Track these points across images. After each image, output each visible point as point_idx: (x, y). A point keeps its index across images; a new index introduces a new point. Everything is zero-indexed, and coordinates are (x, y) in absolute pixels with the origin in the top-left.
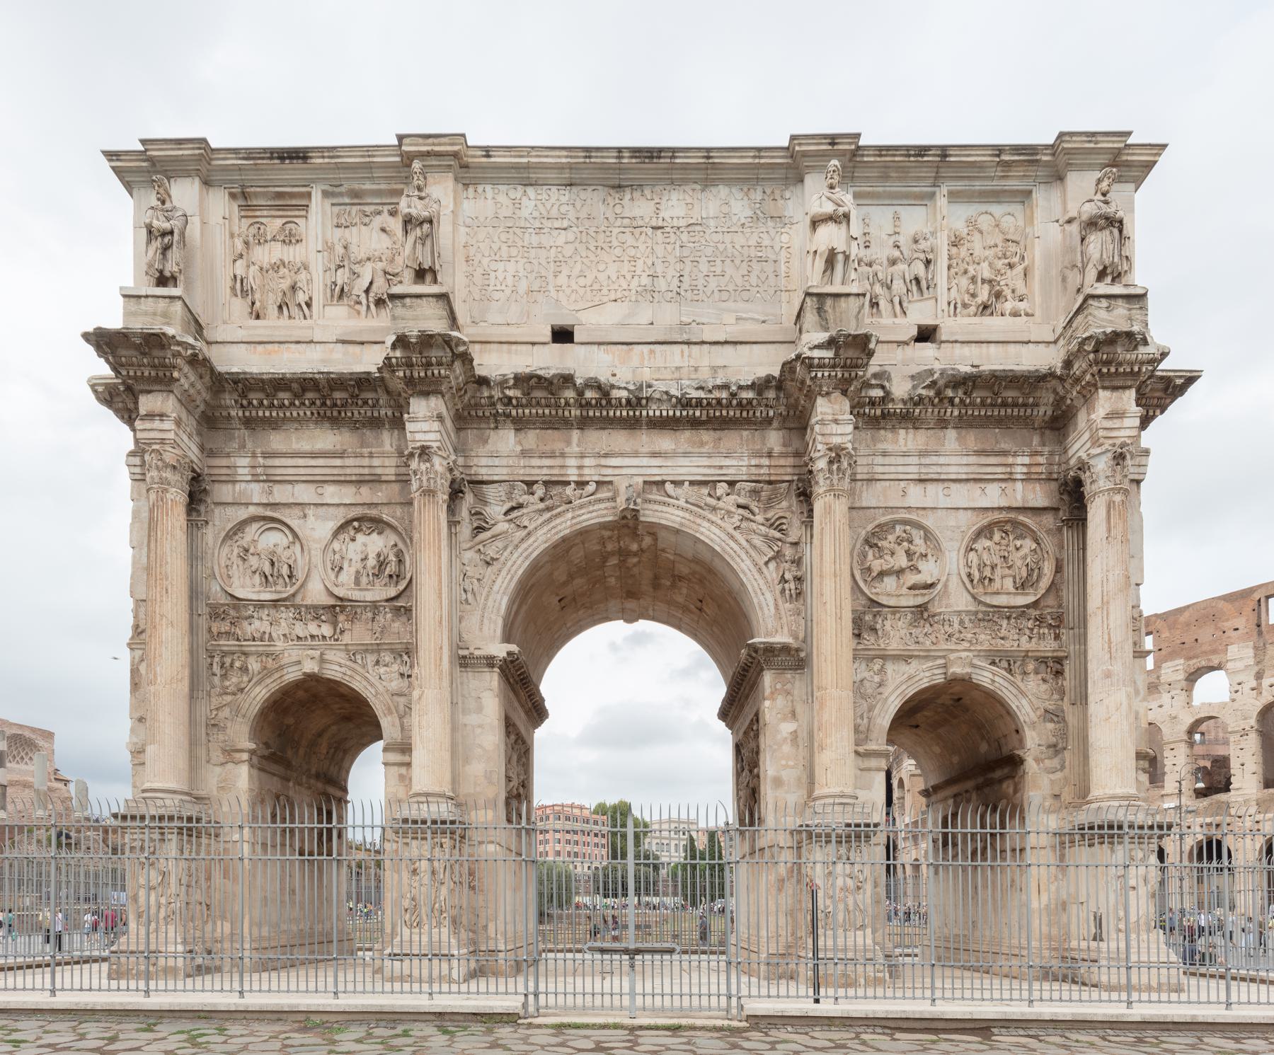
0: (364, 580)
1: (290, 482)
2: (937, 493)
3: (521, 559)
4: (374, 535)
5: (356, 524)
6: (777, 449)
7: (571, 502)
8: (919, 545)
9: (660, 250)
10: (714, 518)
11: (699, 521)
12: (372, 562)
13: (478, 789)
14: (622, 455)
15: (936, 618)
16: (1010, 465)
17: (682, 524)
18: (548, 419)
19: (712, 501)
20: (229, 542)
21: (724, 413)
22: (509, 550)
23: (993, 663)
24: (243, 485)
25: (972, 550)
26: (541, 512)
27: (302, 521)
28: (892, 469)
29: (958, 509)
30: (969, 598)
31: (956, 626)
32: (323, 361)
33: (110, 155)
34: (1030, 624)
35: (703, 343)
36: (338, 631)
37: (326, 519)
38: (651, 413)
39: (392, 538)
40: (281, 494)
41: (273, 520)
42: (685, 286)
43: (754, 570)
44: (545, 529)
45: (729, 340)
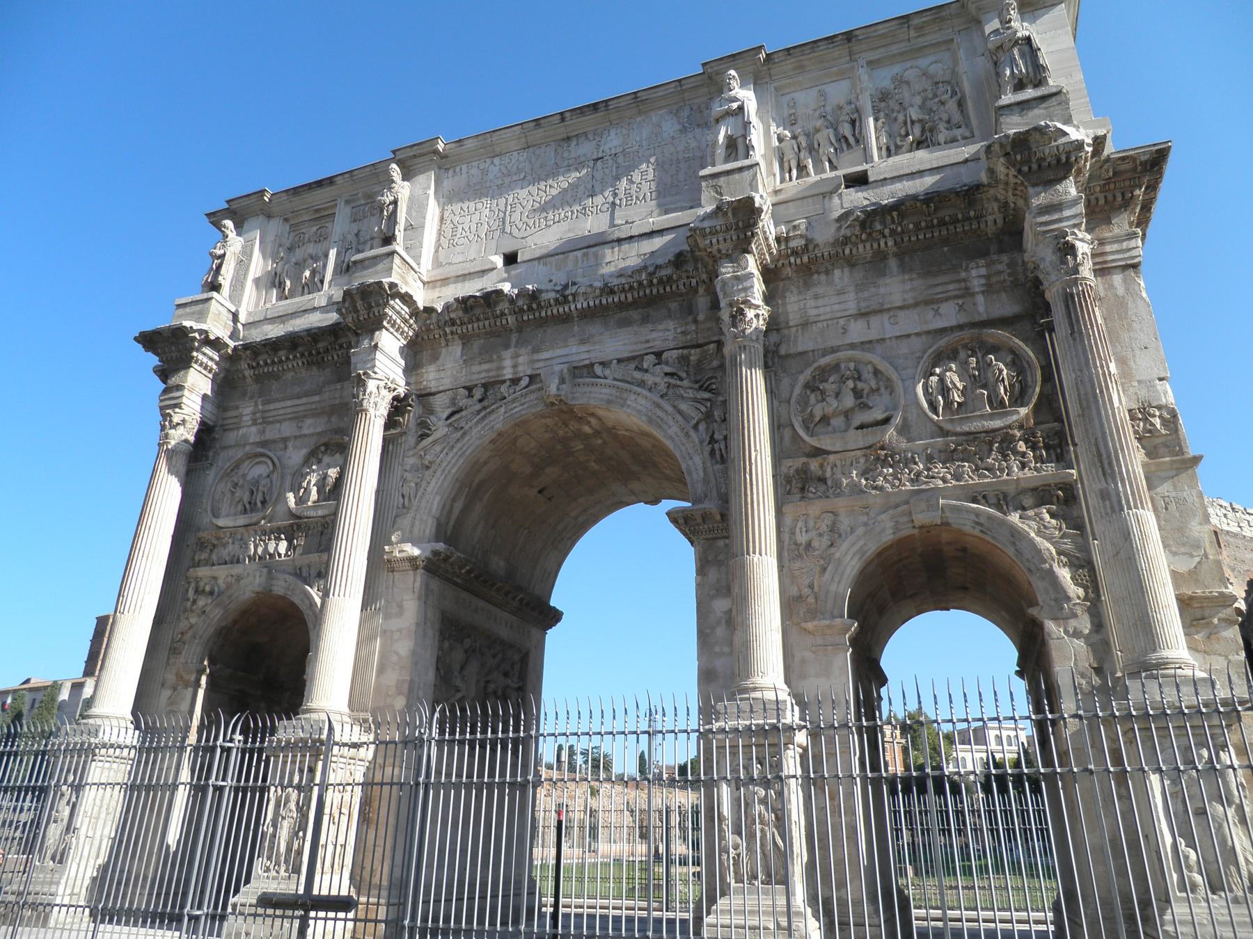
1: (279, 421)
5: (323, 448)
7: (505, 398)
9: (598, 175)
11: (625, 395)
16: (964, 280)
18: (488, 329)
21: (648, 291)
22: (445, 452)
23: (975, 500)
24: (245, 429)
26: (479, 412)
27: (282, 452)
28: (828, 309)
29: (908, 336)
33: (208, 215)
38: (579, 306)
40: (271, 433)
41: (262, 455)
45: (655, 229)
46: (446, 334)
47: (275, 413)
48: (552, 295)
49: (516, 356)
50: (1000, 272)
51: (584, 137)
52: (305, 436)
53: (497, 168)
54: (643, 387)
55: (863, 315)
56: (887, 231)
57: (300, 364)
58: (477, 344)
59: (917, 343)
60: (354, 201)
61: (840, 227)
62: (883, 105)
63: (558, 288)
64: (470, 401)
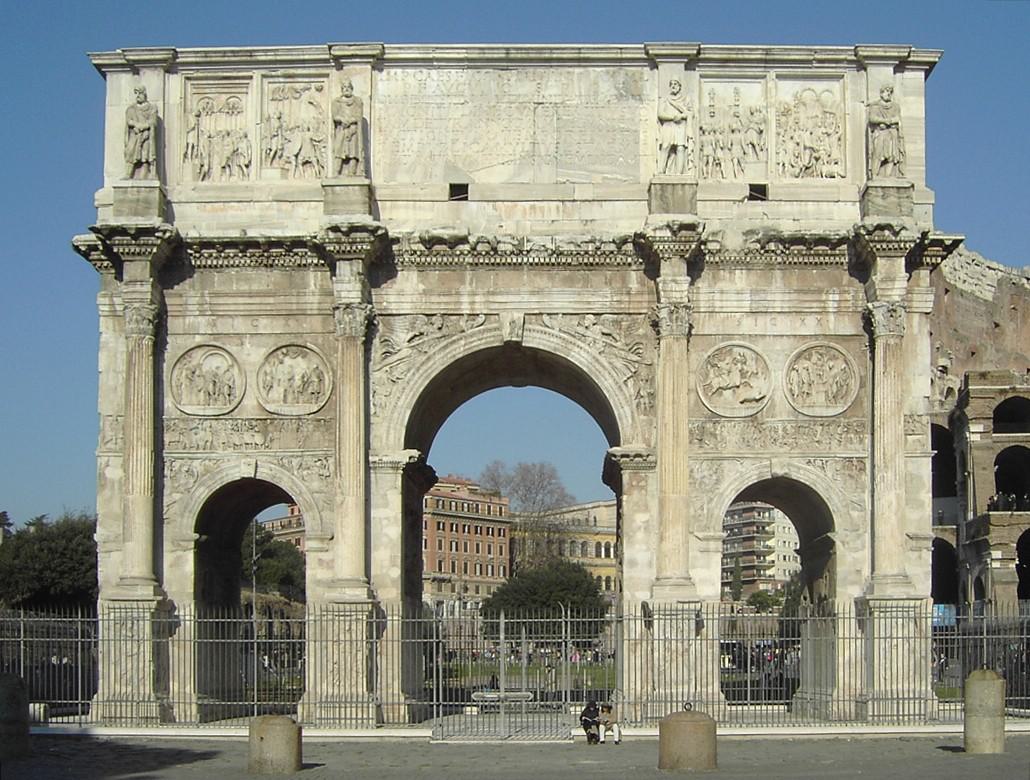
0: (290, 398)
1: (230, 316)
2: (765, 324)
3: (423, 378)
4: (299, 359)
5: (284, 350)
6: (634, 285)
7: (463, 331)
8: (751, 366)
9: (540, 123)
10: (582, 345)
11: (570, 346)
12: (298, 382)
13: (384, 571)
14: (508, 293)
15: (764, 426)
16: (824, 301)
17: (555, 349)
19: (581, 330)
25: (794, 369)
27: (240, 348)
31: (780, 432)
32: (260, 216)
34: (839, 430)
35: (574, 201)
36: (269, 439)
37: (259, 346)
38: (531, 260)
39: (315, 361)
40: (224, 326)
42: (561, 152)
43: (615, 387)
44: (442, 354)
47: (226, 308)
48: (509, 248)
56: (779, 252)
57: (248, 261)
58: (434, 275)
59: (786, 343)
60: (272, 77)
61: (746, 240)
62: (783, 119)
63: (516, 243)
64: (431, 329)
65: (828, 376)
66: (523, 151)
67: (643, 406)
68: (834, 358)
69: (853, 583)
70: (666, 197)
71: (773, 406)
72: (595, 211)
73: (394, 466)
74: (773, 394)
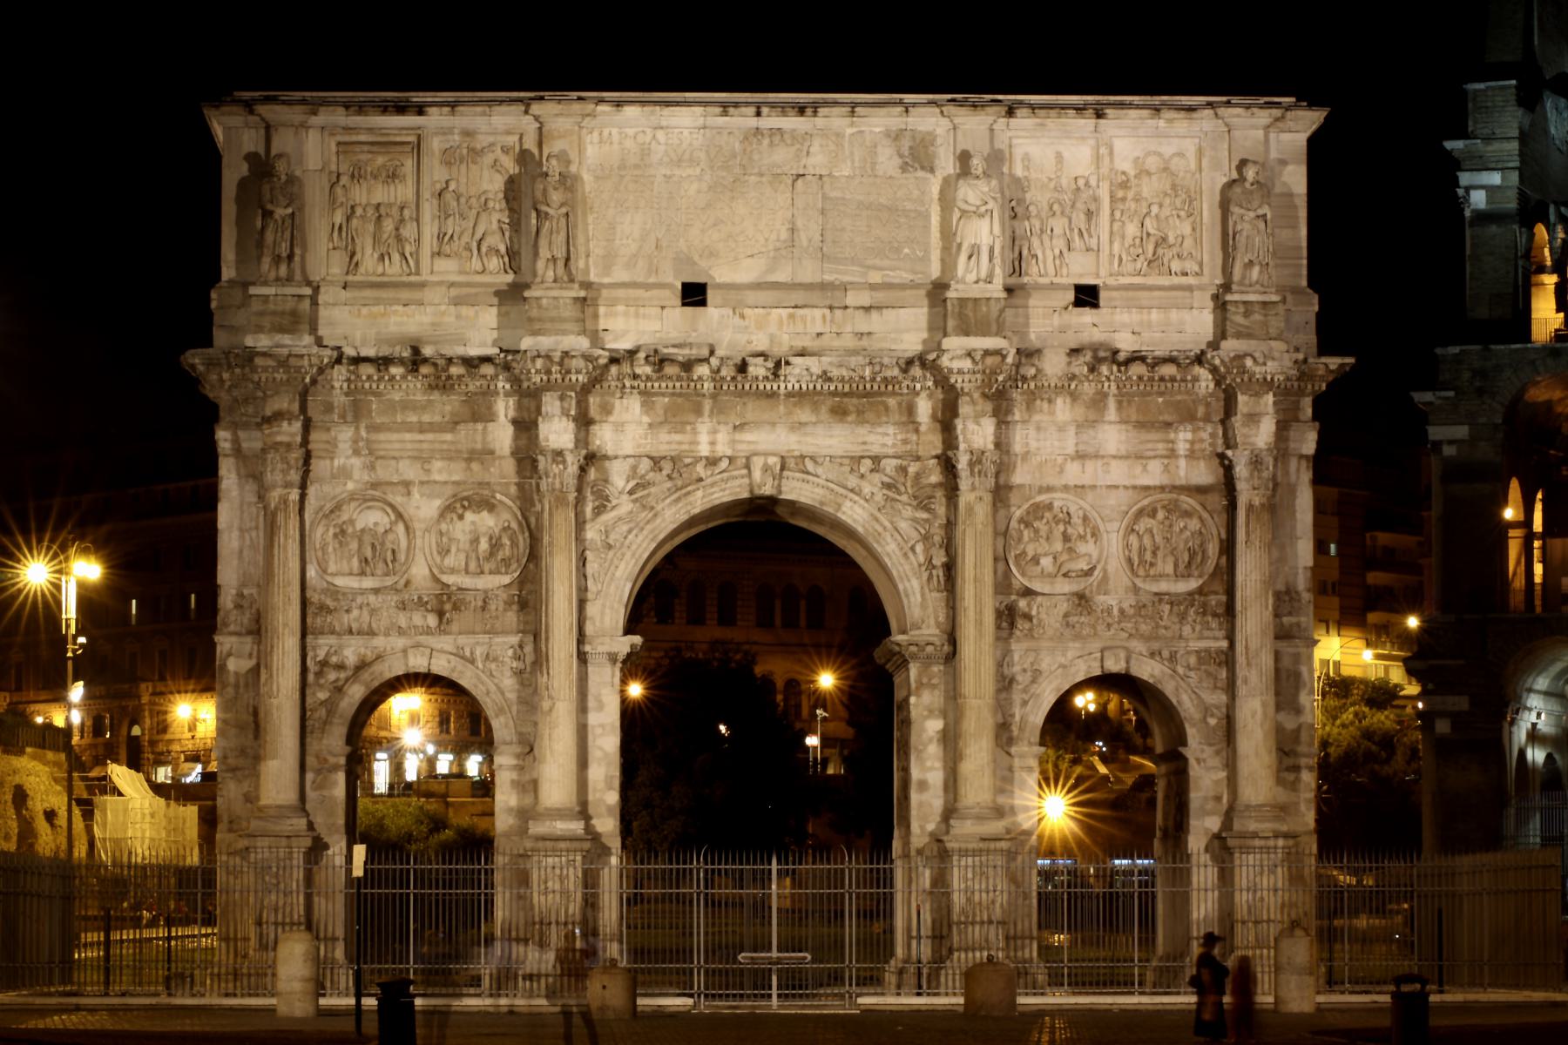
1: (394, 458)
4: (485, 514)
5: (466, 503)
7: (701, 480)
12: (484, 545)
16: (1172, 442)
17: (822, 503)
20: (323, 522)
21: (868, 386)
22: (634, 532)
27: (405, 499)
29: (1117, 487)
30: (1130, 584)
31: (1115, 611)
32: (433, 324)
35: (846, 307)
37: (431, 496)
38: (790, 387)
39: (506, 516)
40: (384, 472)
44: (674, 509)
46: (624, 386)
49: (715, 432)
50: (1202, 441)
51: (778, 137)
52: (436, 482)
53: (662, 148)
54: (858, 494)
55: (1080, 456)
56: (1112, 378)
57: (419, 386)
62: (1120, 194)
65: (1180, 542)
66: (778, 240)
67: (935, 578)
68: (1187, 514)
69: (1211, 813)
70: (966, 315)
71: (1105, 578)
72: (875, 322)
73: (612, 658)
74: (1106, 563)
